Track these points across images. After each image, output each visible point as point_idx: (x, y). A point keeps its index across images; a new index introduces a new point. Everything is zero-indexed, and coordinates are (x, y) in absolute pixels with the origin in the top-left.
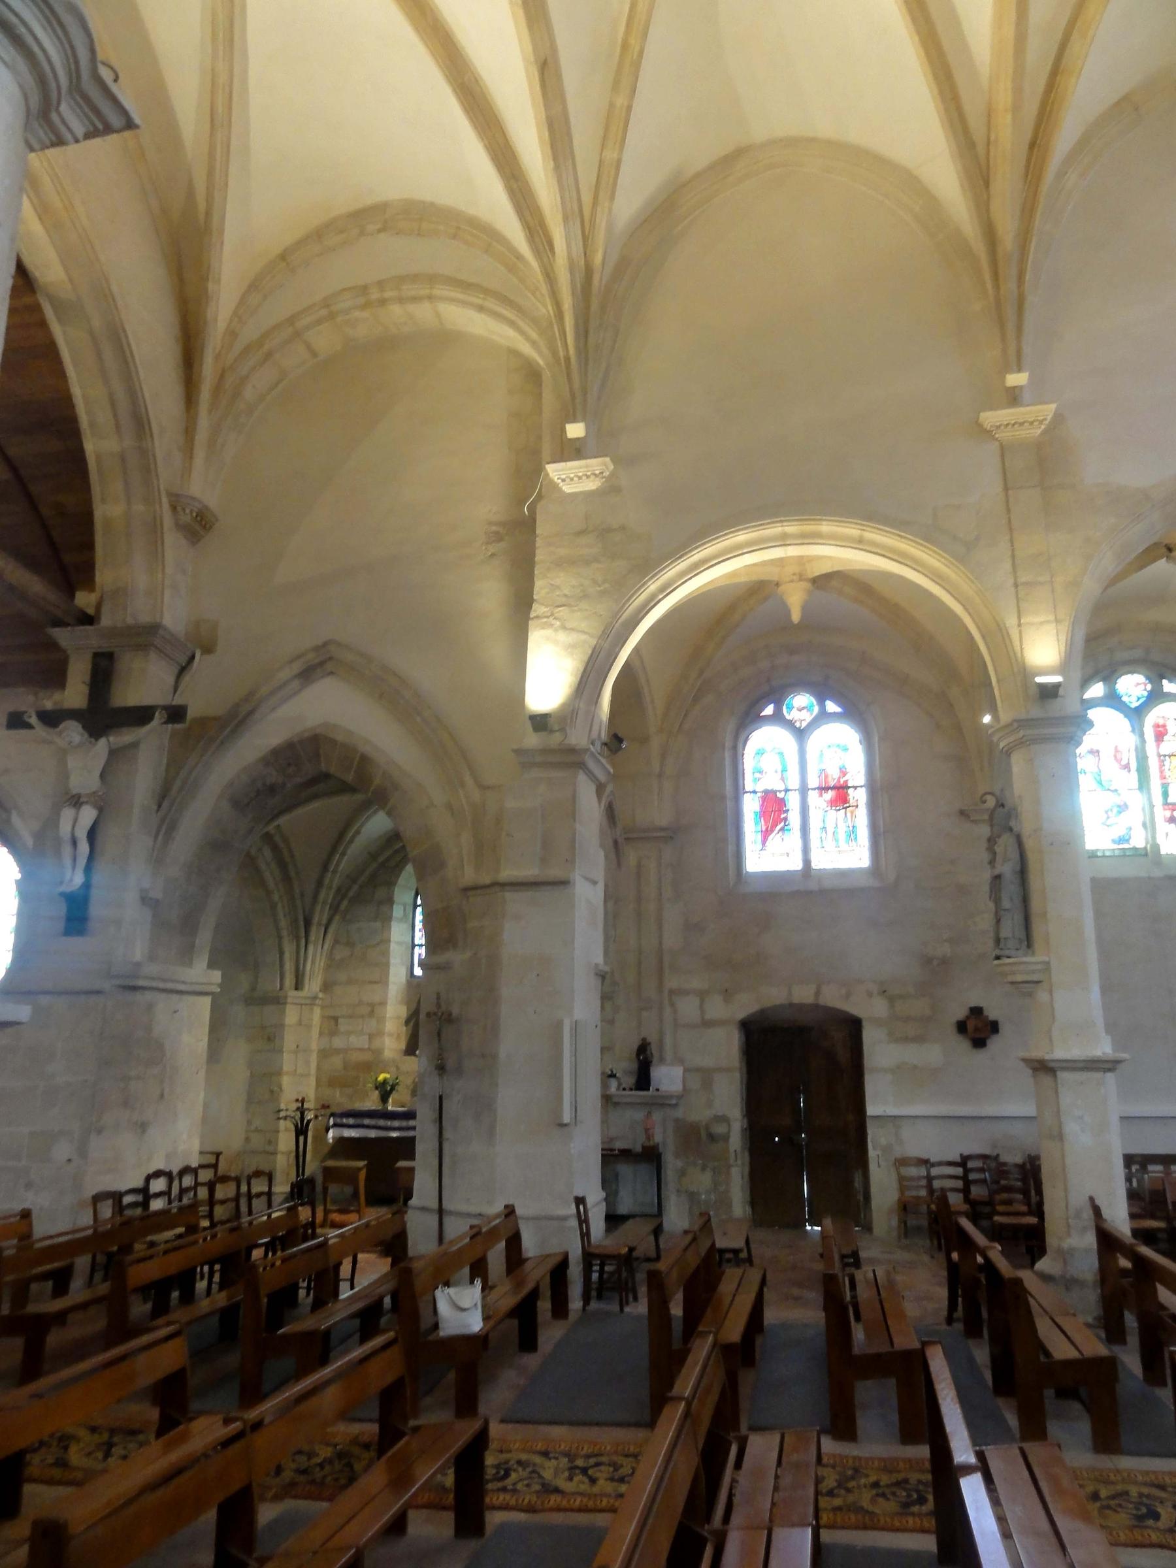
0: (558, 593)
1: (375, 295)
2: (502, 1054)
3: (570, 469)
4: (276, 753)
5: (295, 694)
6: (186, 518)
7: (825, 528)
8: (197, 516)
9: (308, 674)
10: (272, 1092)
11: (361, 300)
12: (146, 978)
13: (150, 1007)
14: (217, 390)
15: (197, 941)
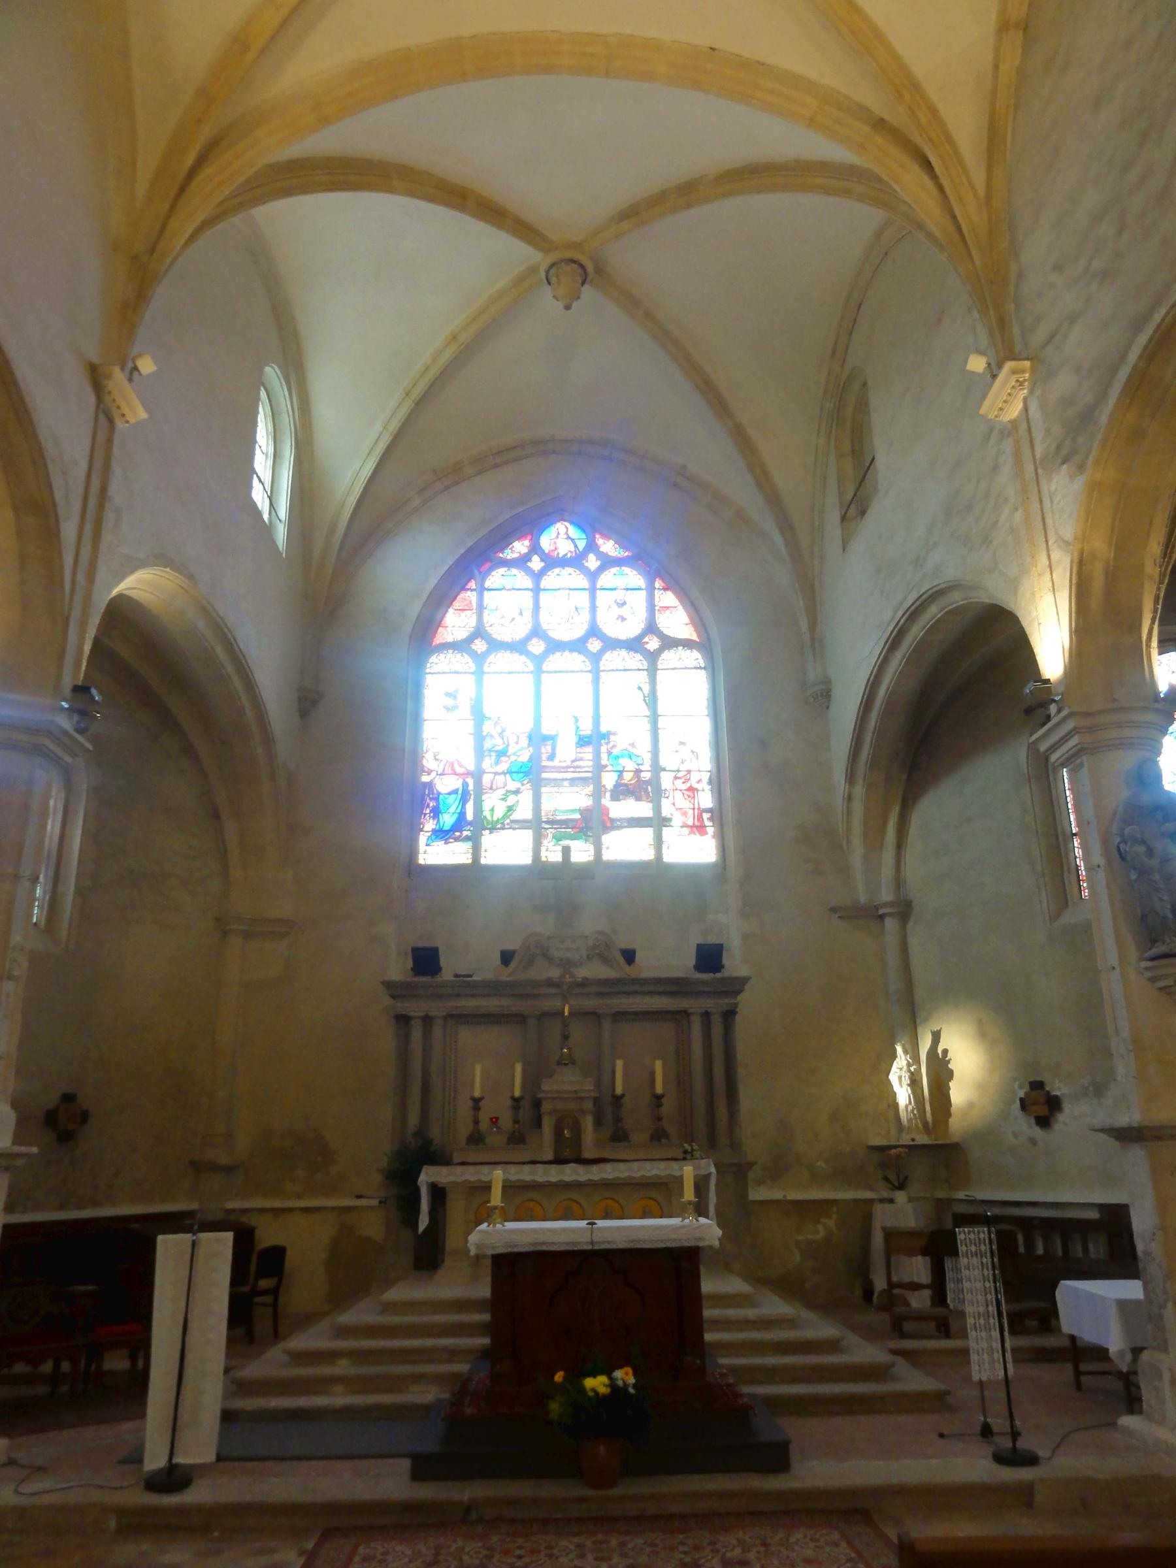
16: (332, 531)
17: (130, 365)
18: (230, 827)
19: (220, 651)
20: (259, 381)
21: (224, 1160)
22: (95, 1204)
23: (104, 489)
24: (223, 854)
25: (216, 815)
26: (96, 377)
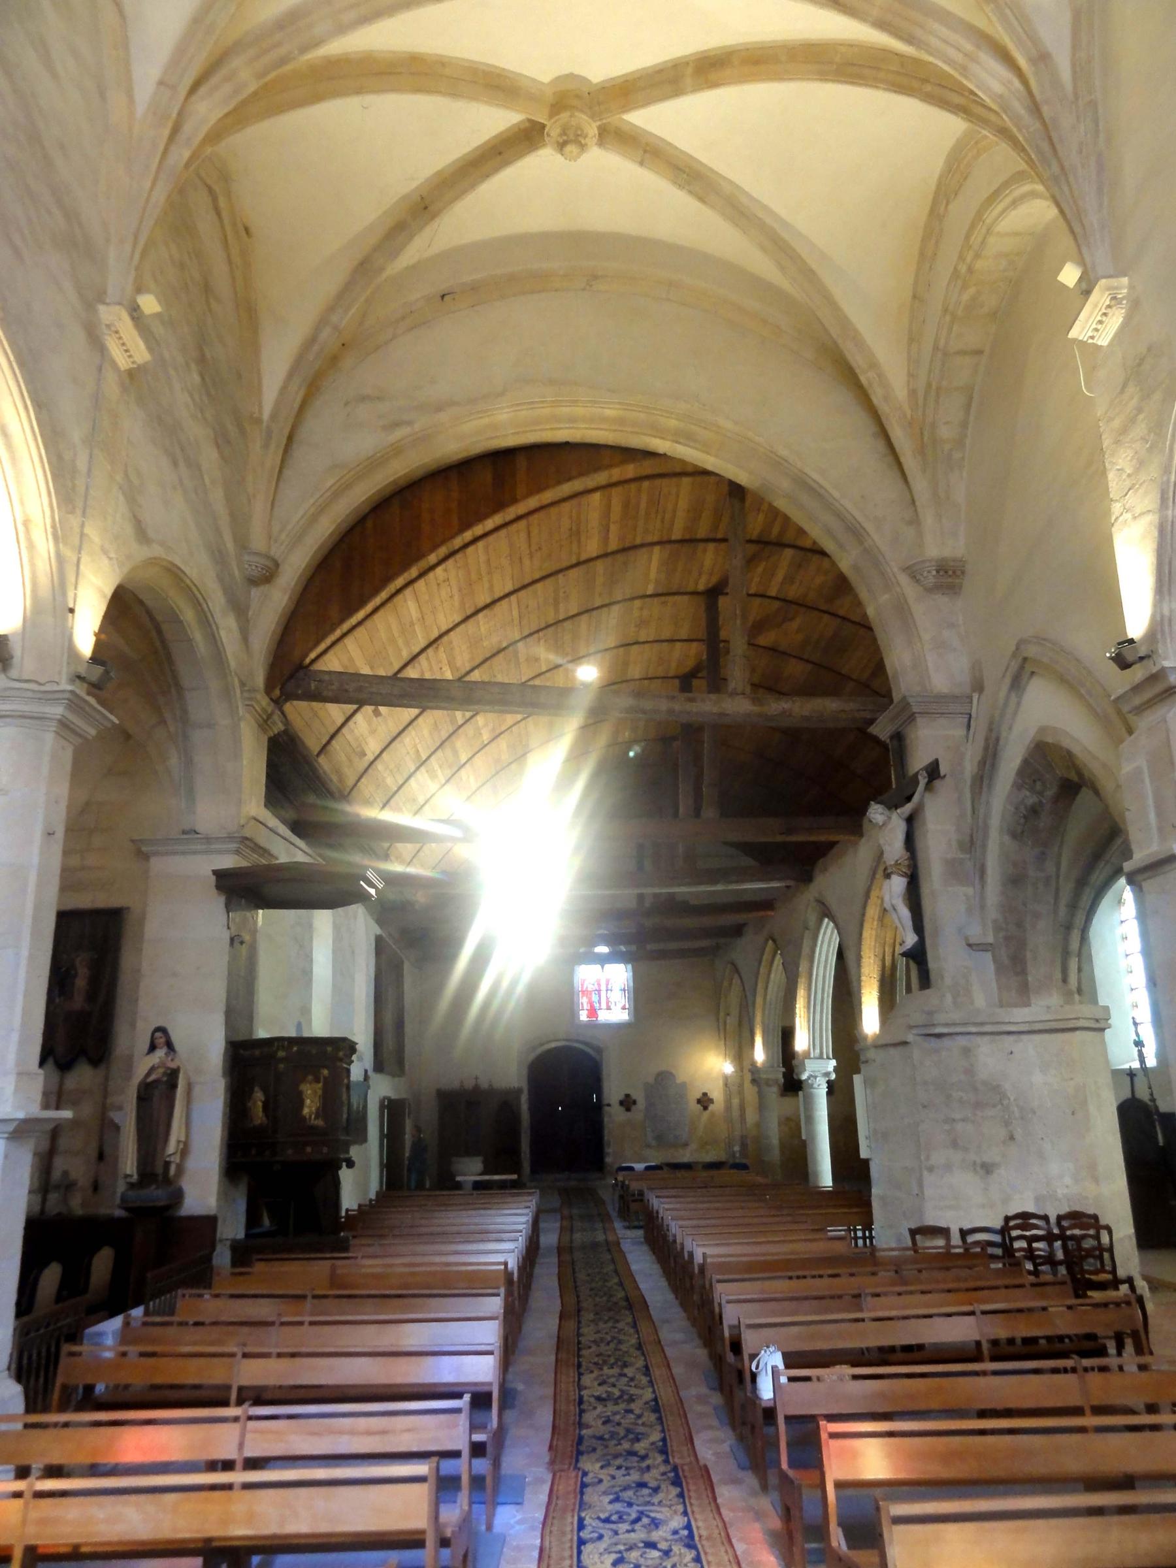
1: (963, 269)
4: (1021, 772)
5: (1019, 704)
6: (931, 580)
8: (938, 572)
9: (1017, 683)
12: (947, 1025)
13: (967, 1051)
14: (921, 450)
15: (1030, 979)
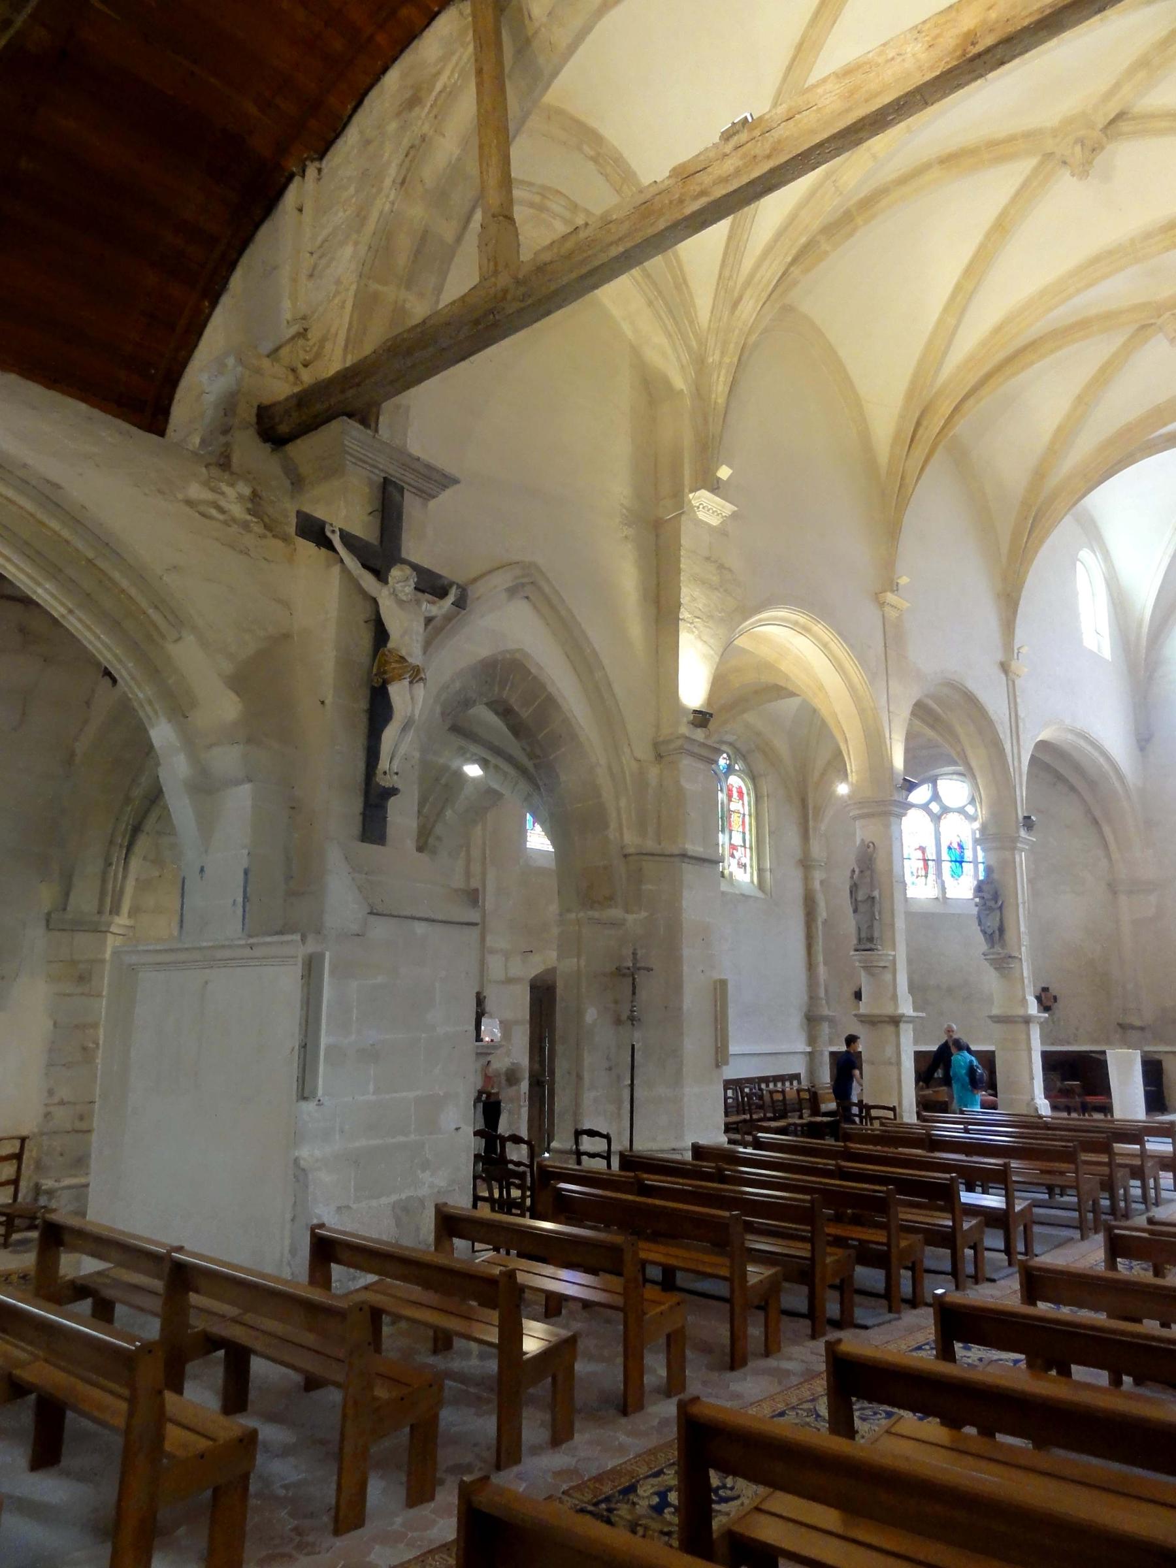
0: (696, 605)
2: (685, 1007)
3: (714, 502)
7: (818, 629)
10: (85, 1049)
11: (568, 215)
16: (1140, 626)
17: (1016, 651)
18: (1107, 830)
19: (1082, 743)
20: (1074, 560)
21: (1138, 1023)
22: (1069, 1043)
23: (1016, 715)
24: (1106, 846)
25: (1095, 822)
26: (1005, 668)
